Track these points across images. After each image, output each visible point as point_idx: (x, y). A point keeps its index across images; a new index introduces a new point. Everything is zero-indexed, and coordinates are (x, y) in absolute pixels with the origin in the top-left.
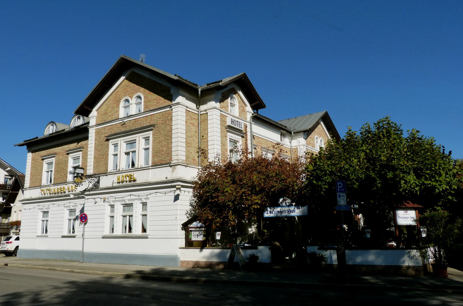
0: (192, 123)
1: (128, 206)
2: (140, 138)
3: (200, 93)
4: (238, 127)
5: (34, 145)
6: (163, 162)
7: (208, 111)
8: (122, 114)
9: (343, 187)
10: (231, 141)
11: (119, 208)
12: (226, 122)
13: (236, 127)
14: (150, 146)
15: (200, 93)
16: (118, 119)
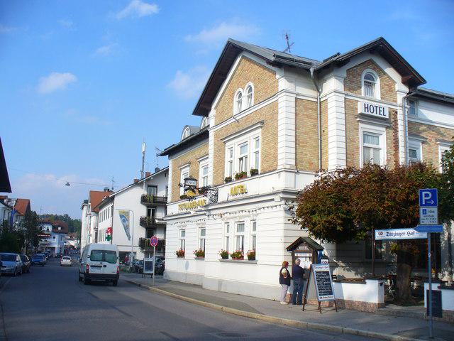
0: (307, 115)
1: (241, 226)
2: (249, 138)
3: (312, 73)
4: (378, 115)
5: (171, 152)
6: (271, 169)
7: (328, 96)
8: (235, 111)
9: (433, 198)
10: (366, 135)
11: (233, 226)
12: (357, 109)
13: (374, 114)
14: (259, 149)
15: (312, 73)
16: (233, 117)
